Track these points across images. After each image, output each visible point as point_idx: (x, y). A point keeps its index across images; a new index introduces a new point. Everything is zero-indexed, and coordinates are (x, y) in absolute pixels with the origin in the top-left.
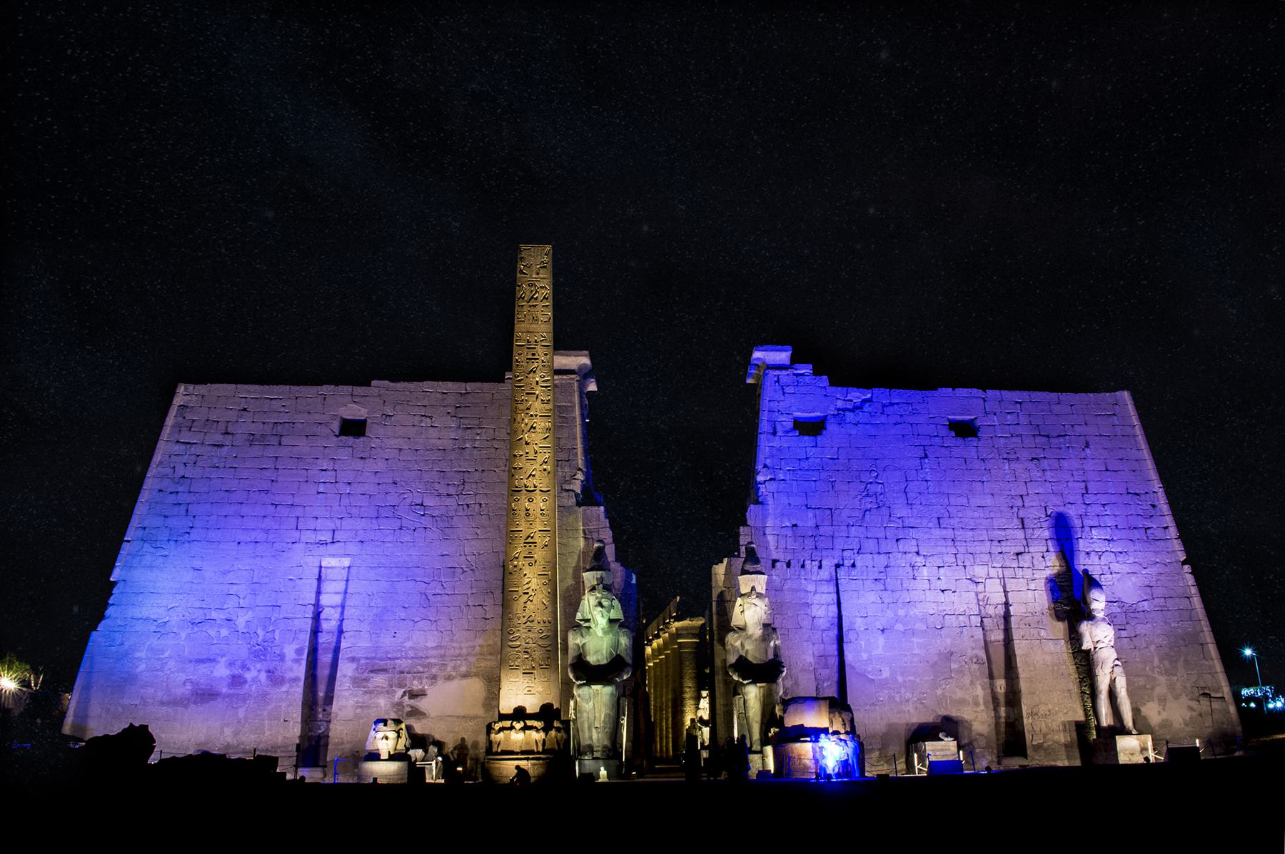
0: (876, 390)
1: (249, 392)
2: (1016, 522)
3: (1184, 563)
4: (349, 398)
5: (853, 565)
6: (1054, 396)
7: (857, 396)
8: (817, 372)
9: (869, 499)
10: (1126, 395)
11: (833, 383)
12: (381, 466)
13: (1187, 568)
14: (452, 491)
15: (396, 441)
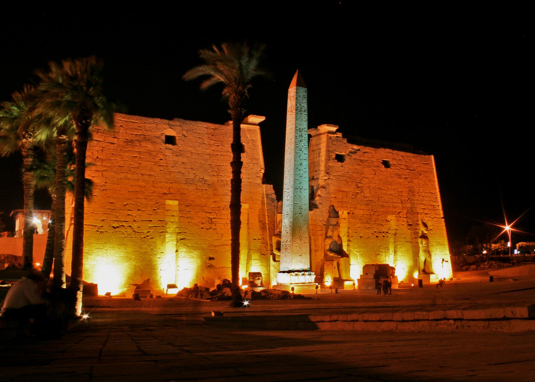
0: (362, 147)
1: (123, 118)
2: (400, 201)
3: (443, 218)
4: (168, 126)
5: (353, 213)
6: (412, 155)
7: (356, 147)
8: (344, 137)
9: (358, 189)
10: (432, 157)
11: (349, 142)
12: (185, 160)
13: (443, 220)
14: (215, 174)
15: (190, 149)
